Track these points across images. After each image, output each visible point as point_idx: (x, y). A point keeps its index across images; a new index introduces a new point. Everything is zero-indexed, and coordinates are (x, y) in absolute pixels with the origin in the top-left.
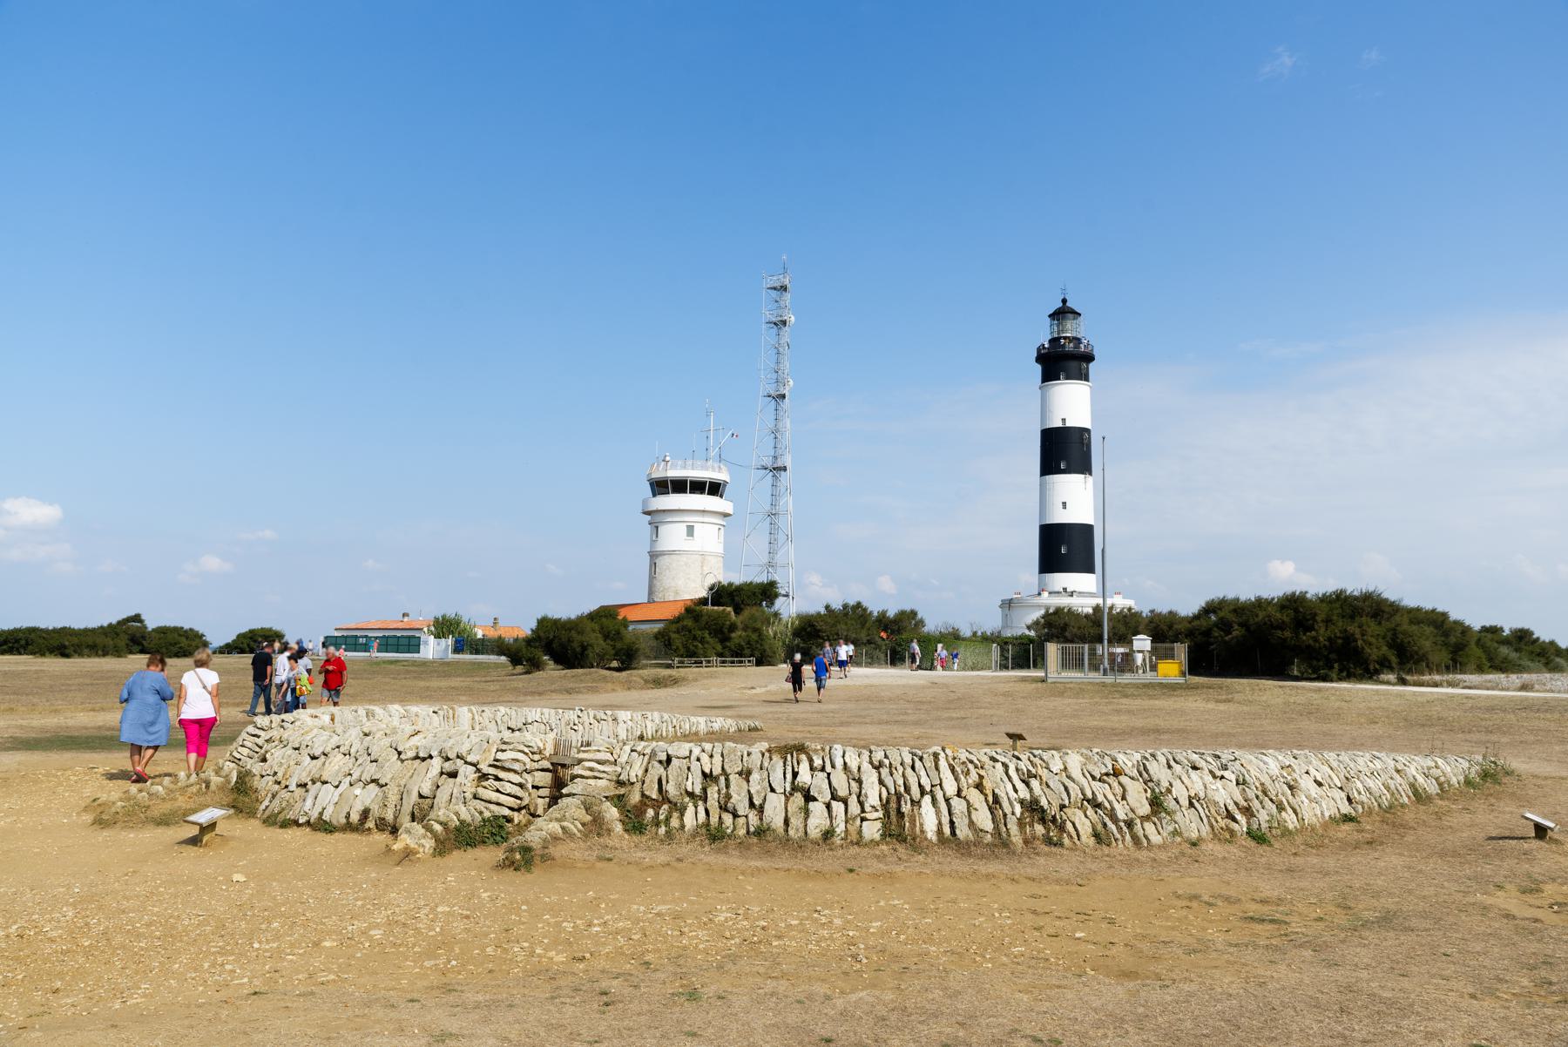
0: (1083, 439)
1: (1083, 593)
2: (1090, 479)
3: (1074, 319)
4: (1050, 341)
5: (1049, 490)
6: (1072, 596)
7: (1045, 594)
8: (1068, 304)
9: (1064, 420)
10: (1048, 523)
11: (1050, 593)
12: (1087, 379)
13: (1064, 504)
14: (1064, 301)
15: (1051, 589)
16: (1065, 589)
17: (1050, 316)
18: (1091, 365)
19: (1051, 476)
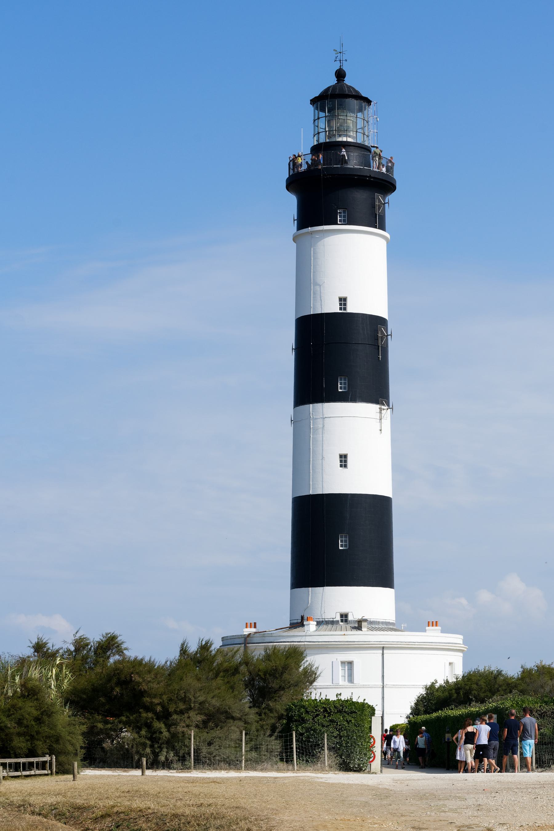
0: (377, 338)
1: (378, 623)
2: (387, 413)
3: (361, 110)
4: (316, 150)
5: (316, 430)
6: (359, 628)
7: (311, 626)
8: (348, 81)
9: (343, 301)
10: (311, 493)
11: (319, 623)
12: (382, 227)
13: (344, 460)
14: (340, 75)
15: (320, 618)
16: (344, 617)
17: (314, 101)
18: (391, 198)
19: (320, 405)
